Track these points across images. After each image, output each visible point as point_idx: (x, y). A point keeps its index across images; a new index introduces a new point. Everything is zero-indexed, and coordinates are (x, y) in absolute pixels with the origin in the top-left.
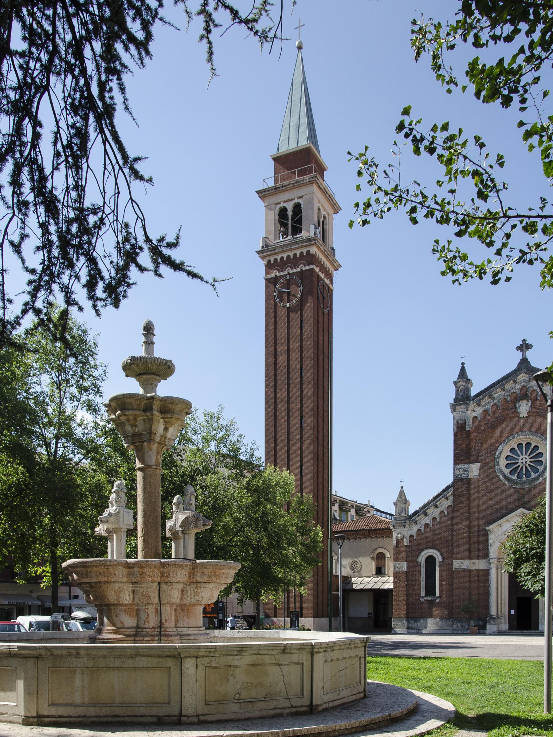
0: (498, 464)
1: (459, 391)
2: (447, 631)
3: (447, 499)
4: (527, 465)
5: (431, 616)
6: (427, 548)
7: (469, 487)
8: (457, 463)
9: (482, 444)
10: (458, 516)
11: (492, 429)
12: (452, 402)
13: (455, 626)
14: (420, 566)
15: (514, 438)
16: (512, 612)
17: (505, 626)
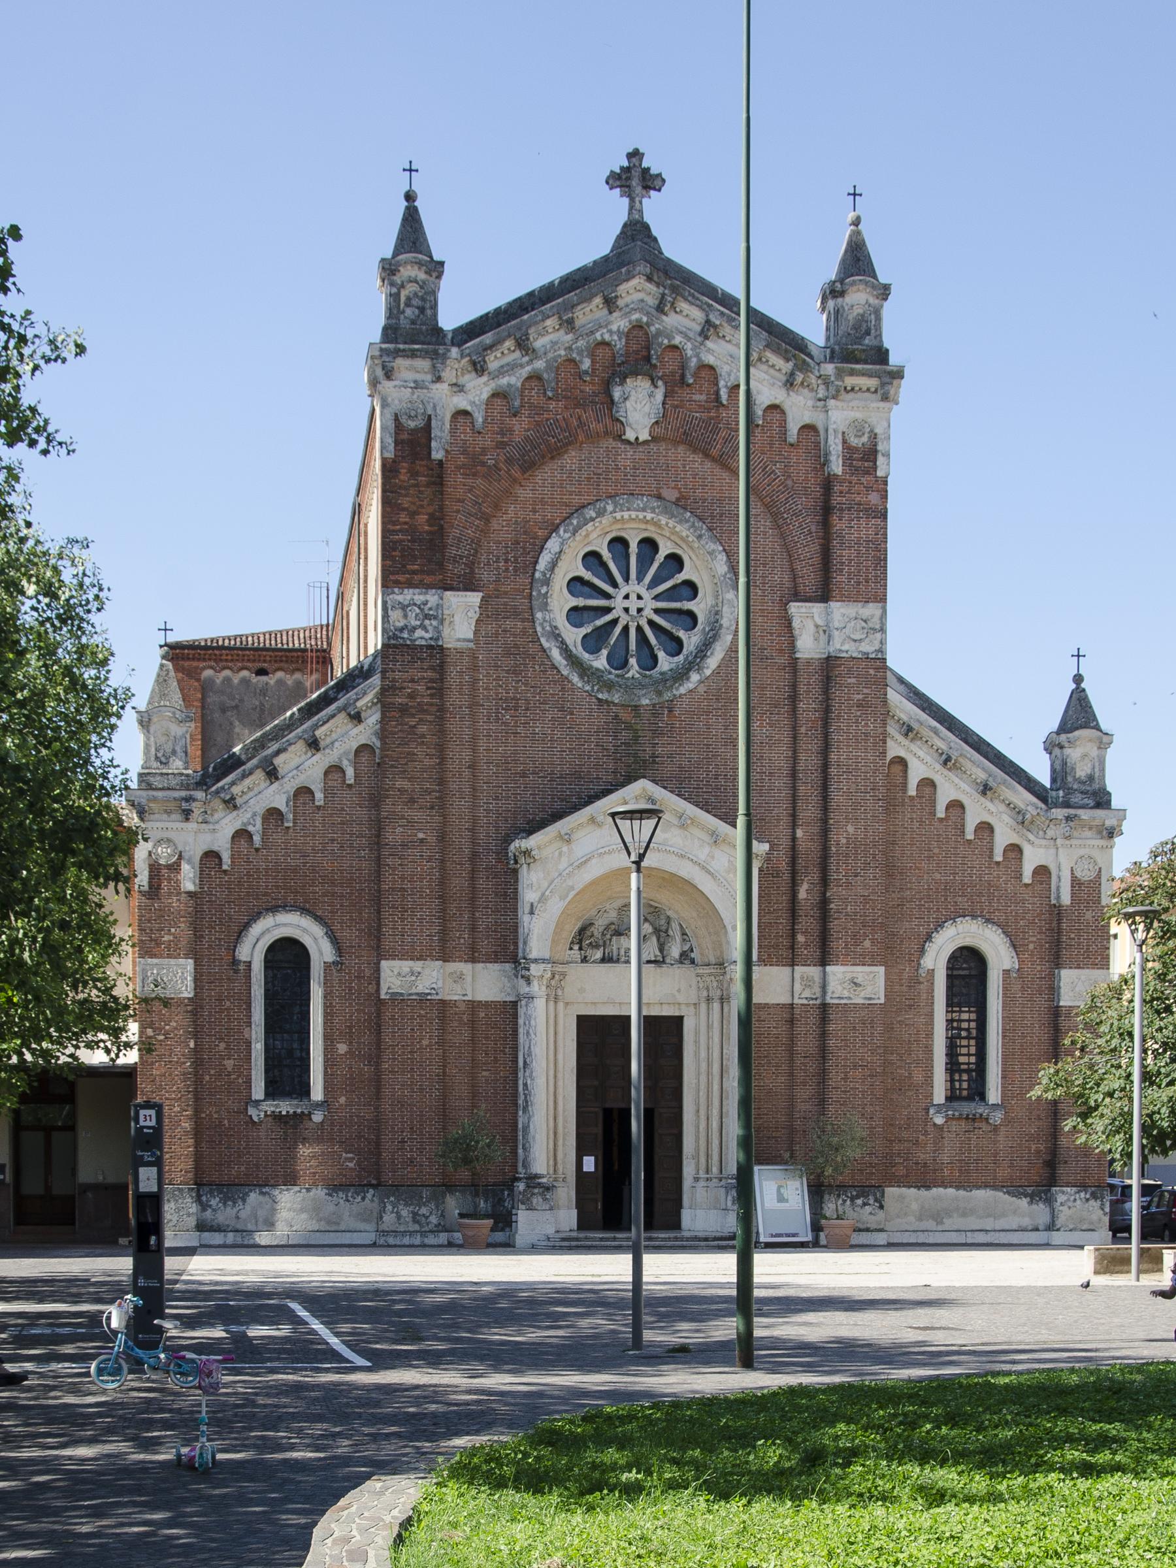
0: (545, 607)
1: (403, 299)
2: (357, 1239)
3: (357, 718)
4: (643, 623)
5: (290, 1179)
6: (274, 909)
7: (442, 680)
8: (397, 583)
9: (487, 519)
10: (402, 791)
11: (524, 470)
12: (376, 336)
13: (389, 1219)
14: (248, 977)
15: (601, 513)
16: (589, 1164)
17: (568, 1218)
